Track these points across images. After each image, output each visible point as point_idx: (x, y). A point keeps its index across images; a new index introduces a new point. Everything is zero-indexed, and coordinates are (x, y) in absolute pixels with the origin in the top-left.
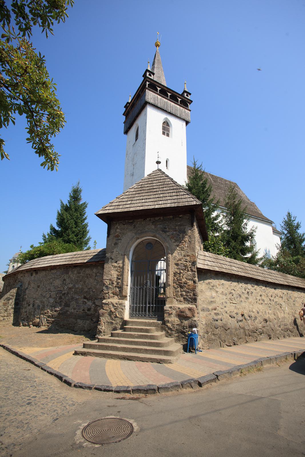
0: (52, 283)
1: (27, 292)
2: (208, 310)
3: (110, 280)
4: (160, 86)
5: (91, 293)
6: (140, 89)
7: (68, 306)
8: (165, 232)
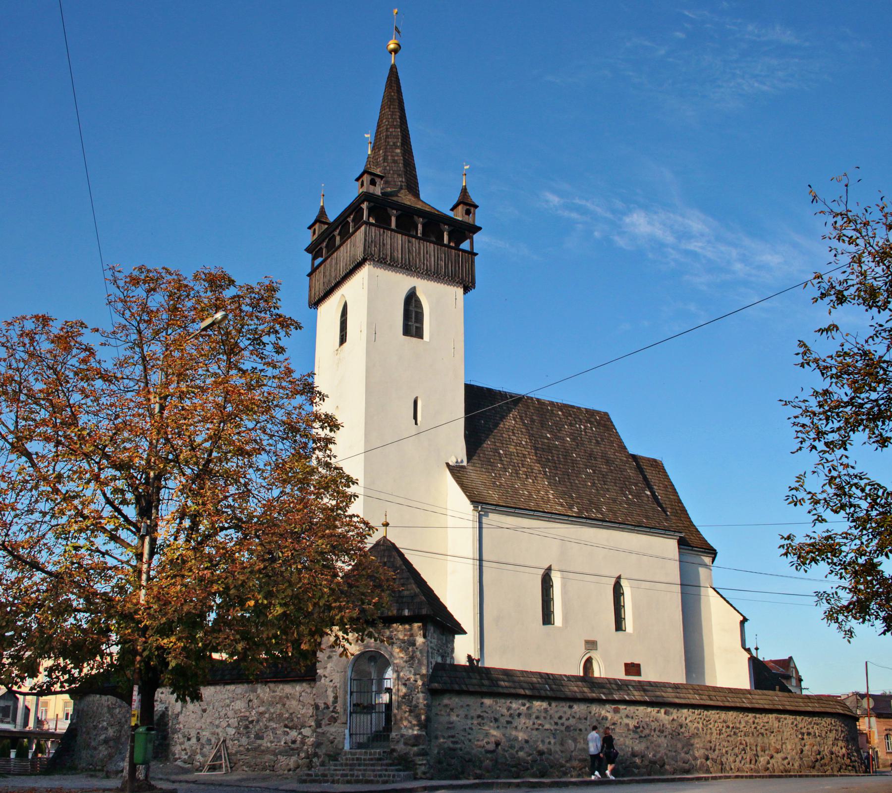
0: (228, 706)
1: (181, 718)
3: (325, 703)
5: (295, 719)
7: (262, 738)
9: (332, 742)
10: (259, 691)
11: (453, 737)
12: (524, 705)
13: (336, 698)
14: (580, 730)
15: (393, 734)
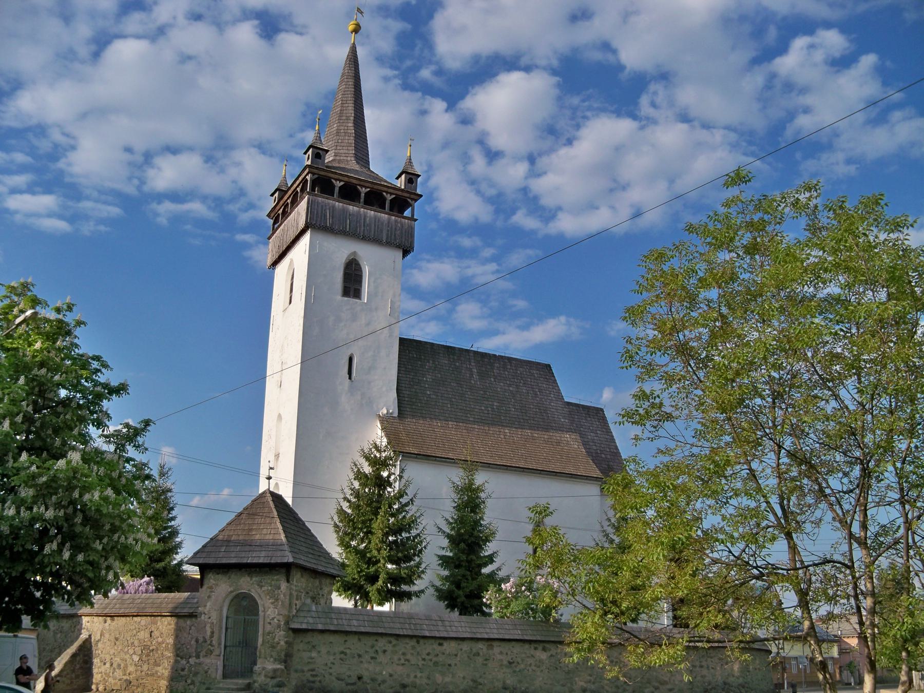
1: (100, 645)
2: (303, 671)
4: (341, 178)
6: (298, 182)
8: (261, 587)
9: (206, 672)
10: (159, 623)
11: (313, 670)
12: (390, 642)
13: (212, 633)
14: (450, 665)
15: (256, 668)
